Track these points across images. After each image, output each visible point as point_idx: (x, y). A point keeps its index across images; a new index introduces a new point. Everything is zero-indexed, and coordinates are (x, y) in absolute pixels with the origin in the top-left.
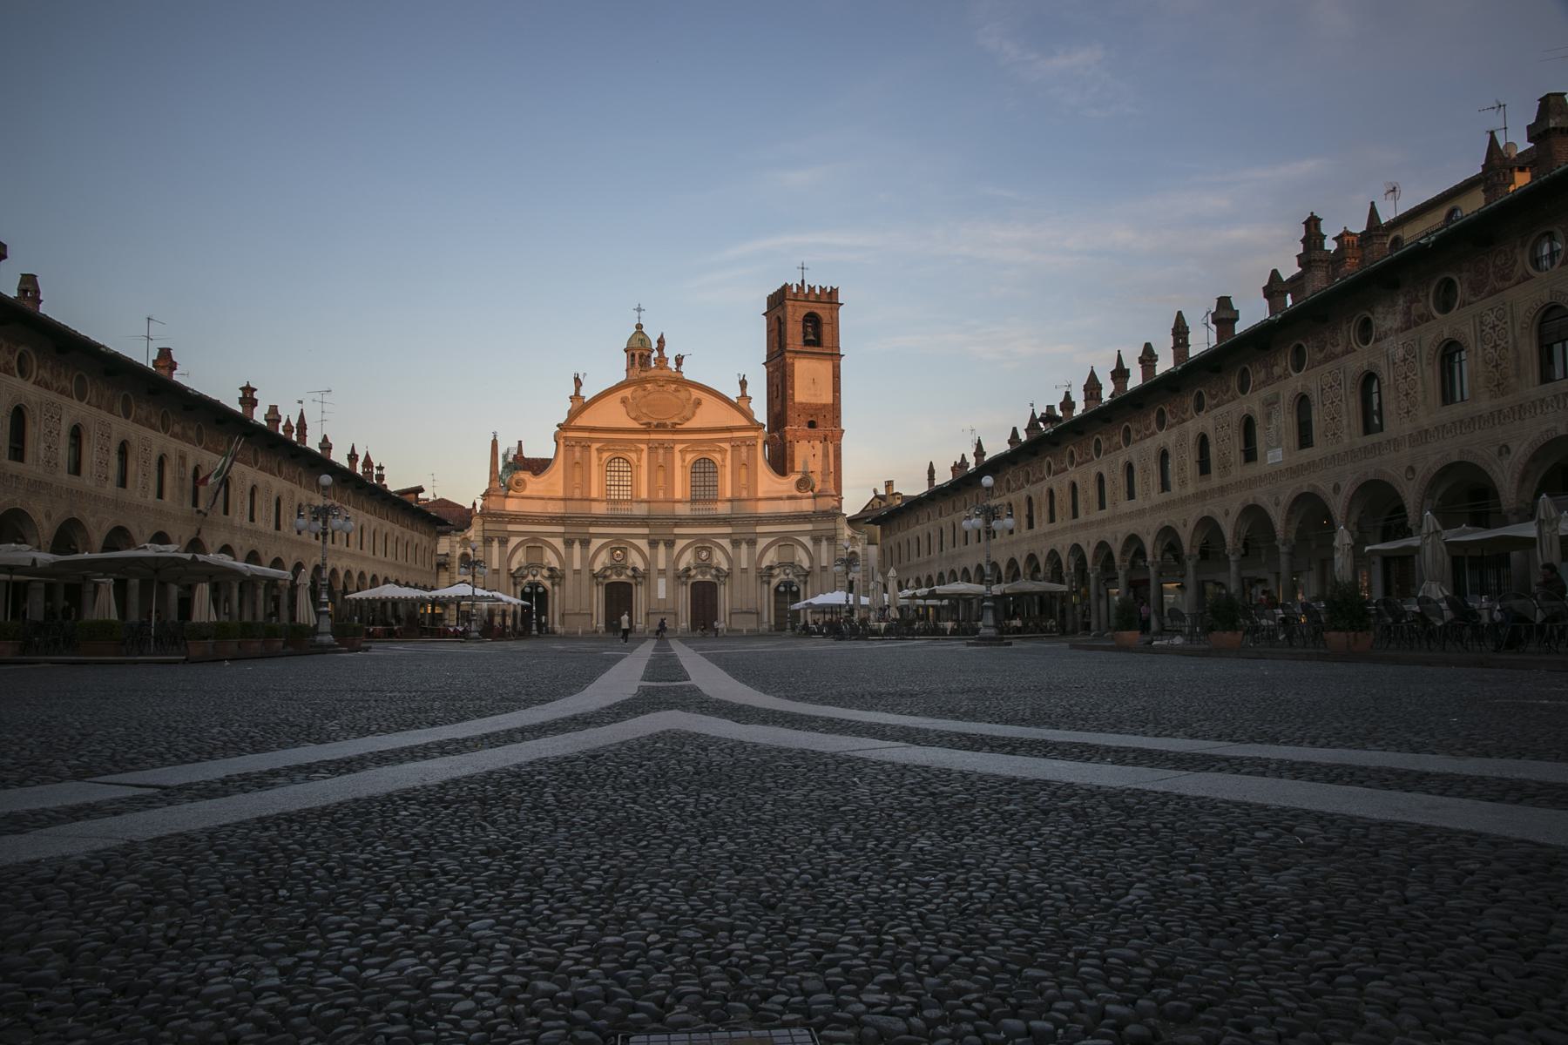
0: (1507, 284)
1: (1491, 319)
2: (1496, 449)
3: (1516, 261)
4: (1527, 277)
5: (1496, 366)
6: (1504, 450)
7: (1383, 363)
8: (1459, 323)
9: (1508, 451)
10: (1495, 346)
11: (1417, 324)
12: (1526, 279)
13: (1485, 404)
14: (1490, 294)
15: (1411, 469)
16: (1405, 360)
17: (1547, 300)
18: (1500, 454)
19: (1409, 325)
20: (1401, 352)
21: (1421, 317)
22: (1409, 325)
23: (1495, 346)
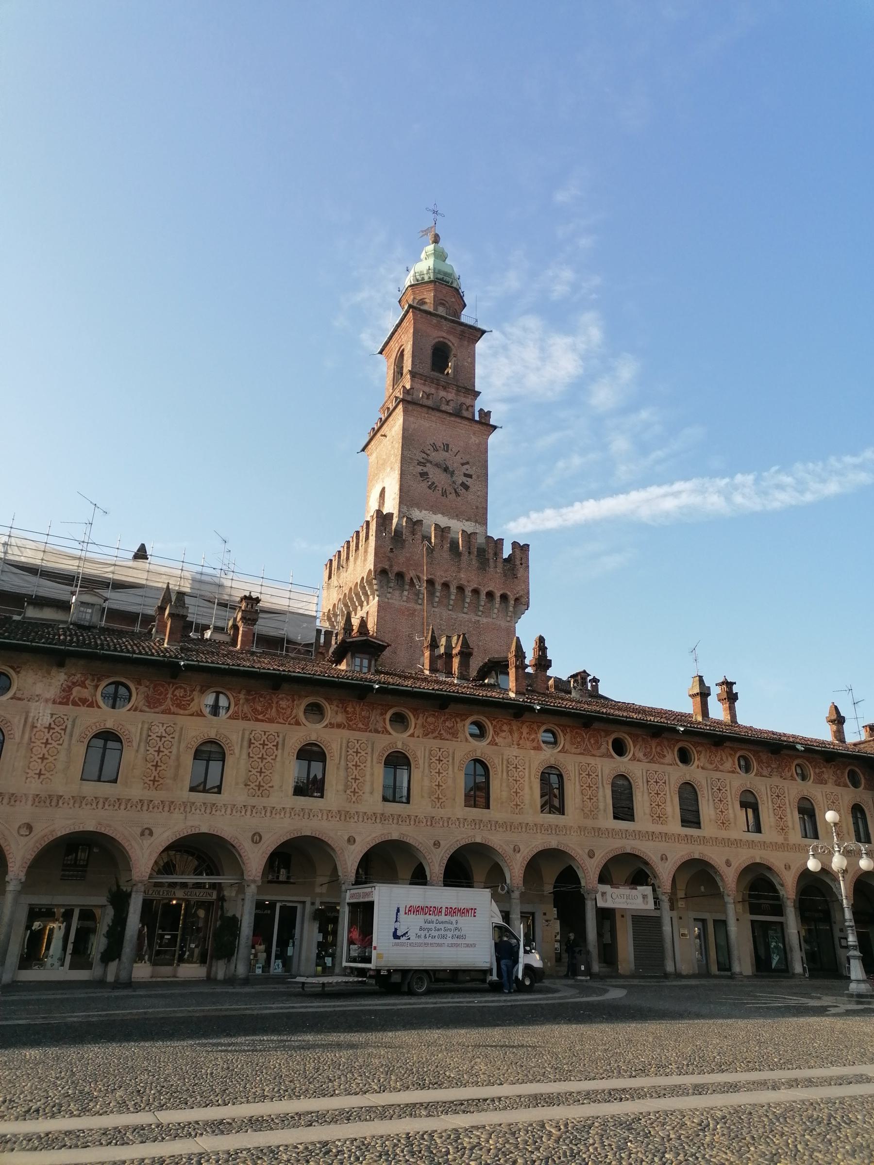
0: (182, 712)
1: (161, 730)
2: (139, 830)
3: (193, 700)
4: (200, 714)
5: (156, 766)
6: (147, 832)
7: (17, 722)
8: (122, 719)
9: (151, 834)
10: (159, 751)
11: (75, 704)
12: (198, 715)
13: (136, 791)
14: (163, 712)
15: (30, 828)
16: (49, 728)
17: (213, 735)
18: (142, 834)
19: (65, 699)
20: (47, 720)
21: (84, 701)
22: (65, 699)
23: (159, 751)
